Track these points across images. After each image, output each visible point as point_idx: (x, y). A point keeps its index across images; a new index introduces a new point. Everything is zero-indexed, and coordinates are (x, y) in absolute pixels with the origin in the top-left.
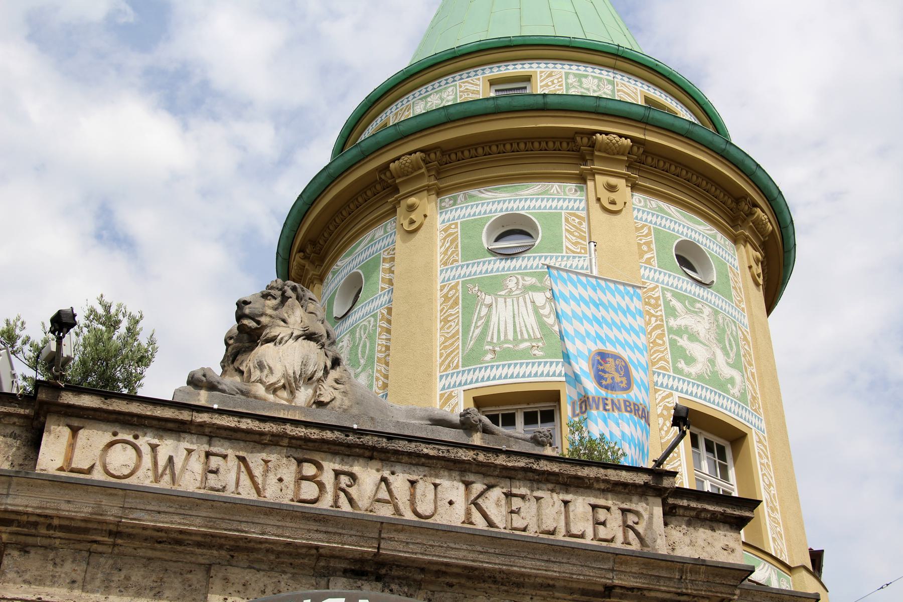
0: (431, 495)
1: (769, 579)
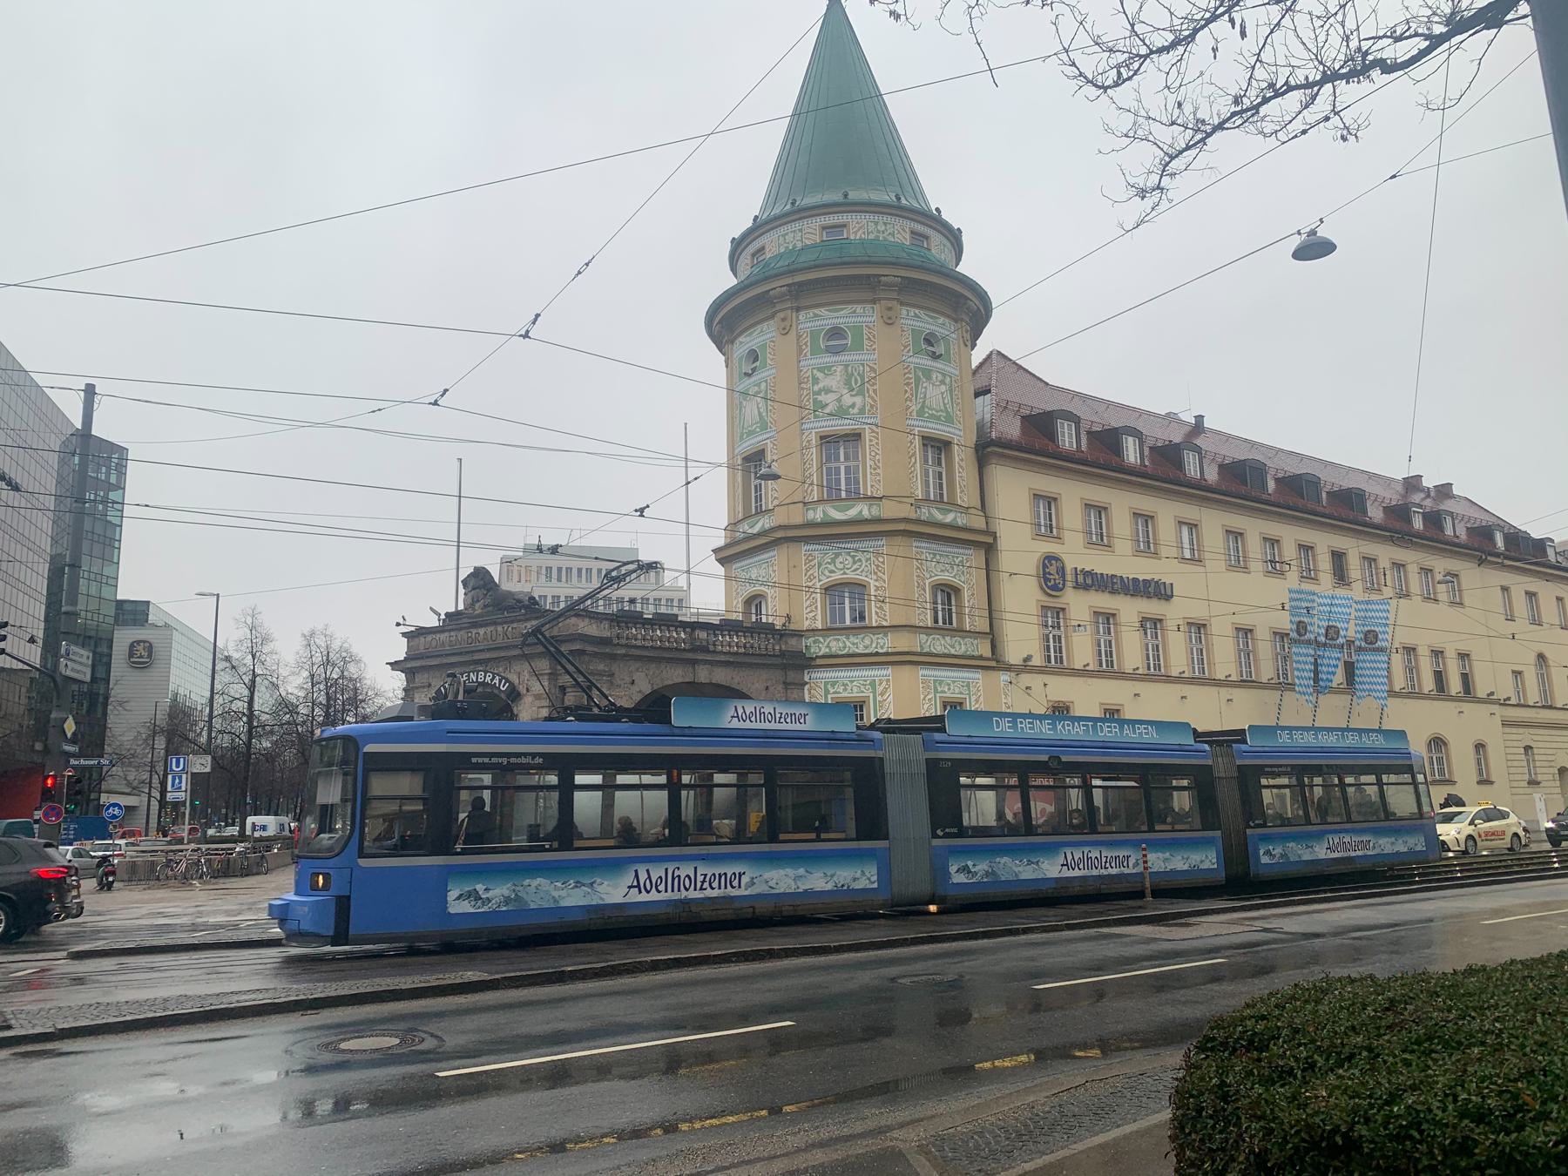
1: (861, 512)
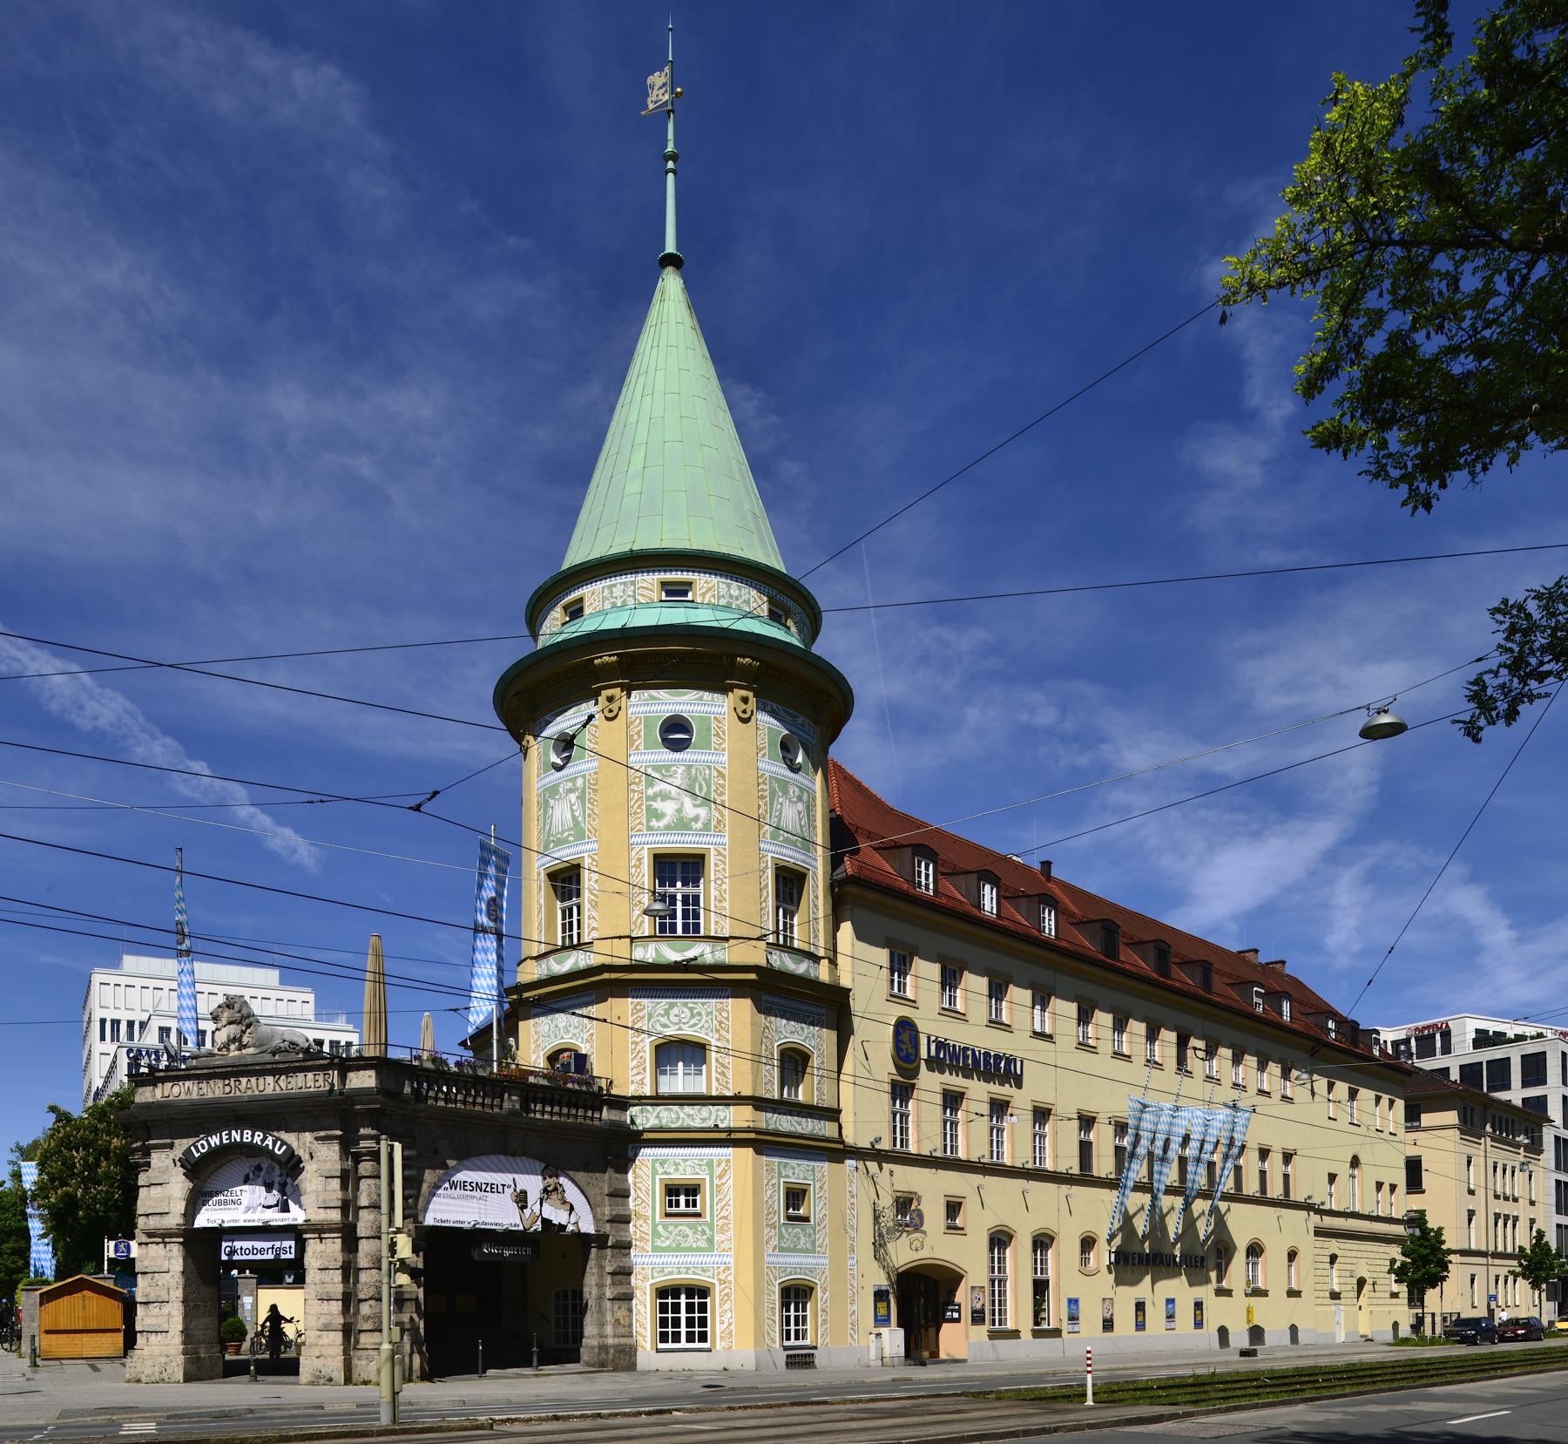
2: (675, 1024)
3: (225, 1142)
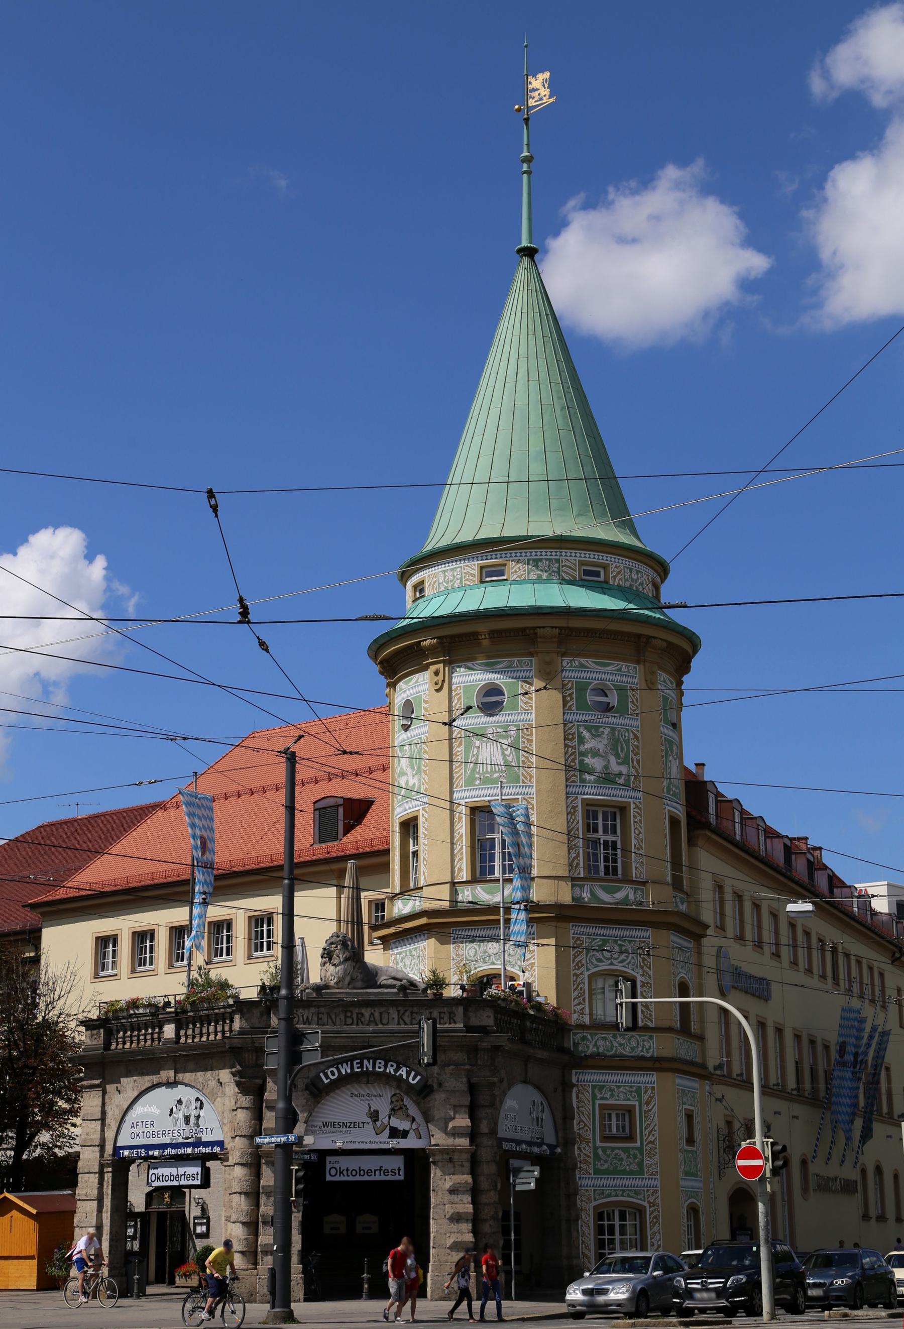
0: (387, 1017)
1: (627, 896)
2: (608, 959)
3: (356, 1070)
